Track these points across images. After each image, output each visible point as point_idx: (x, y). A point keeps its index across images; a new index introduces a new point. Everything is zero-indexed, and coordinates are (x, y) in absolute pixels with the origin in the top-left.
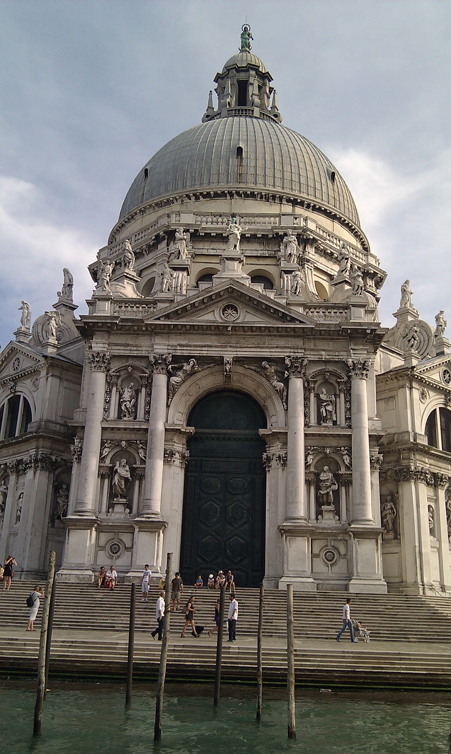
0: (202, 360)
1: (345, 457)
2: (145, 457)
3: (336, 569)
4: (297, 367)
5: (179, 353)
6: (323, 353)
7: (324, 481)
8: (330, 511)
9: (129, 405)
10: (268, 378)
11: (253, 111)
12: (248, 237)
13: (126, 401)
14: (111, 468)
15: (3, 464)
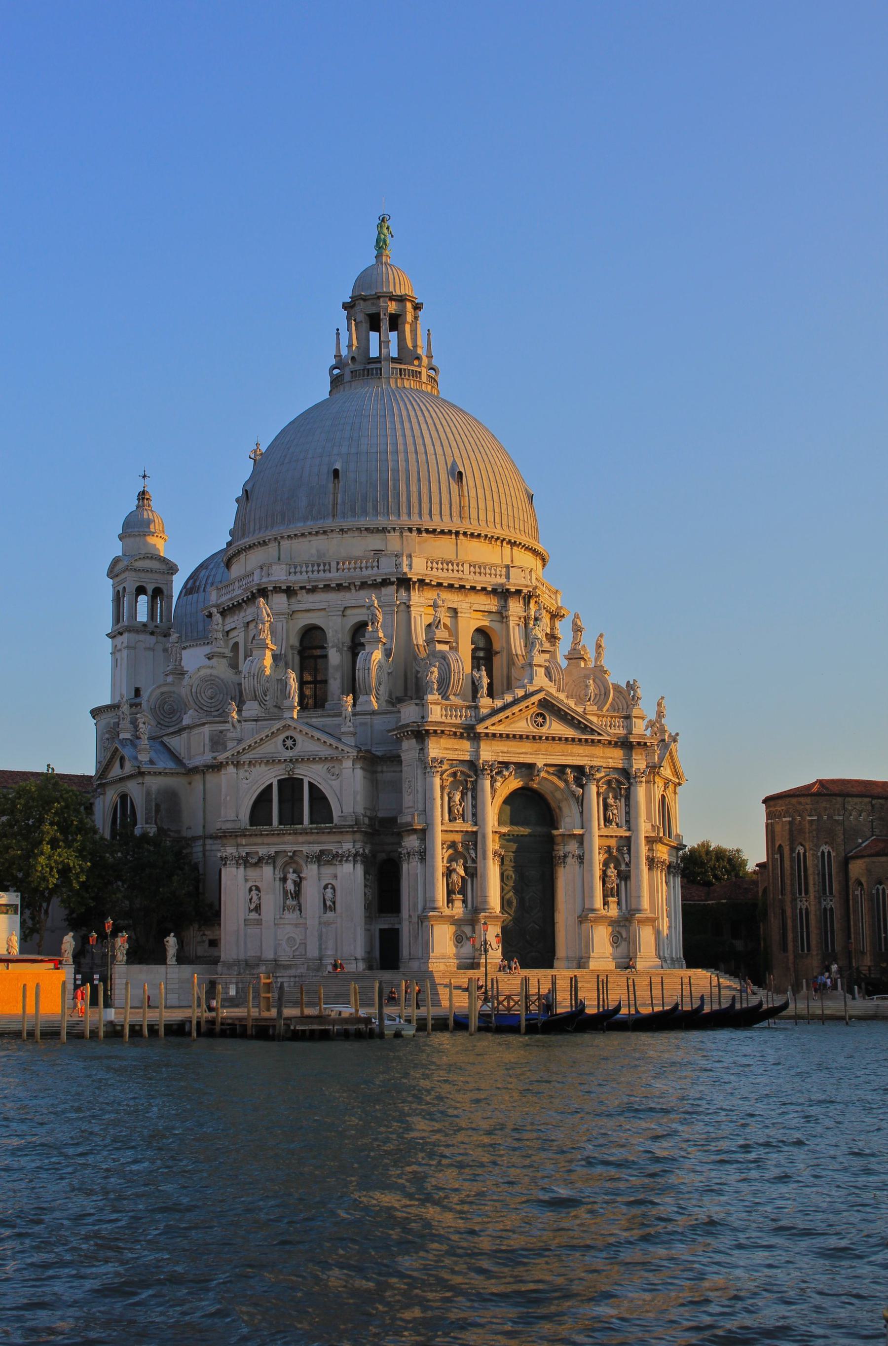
0: (519, 766)
1: (626, 856)
2: (476, 857)
3: (619, 950)
4: (593, 775)
5: (501, 759)
6: (610, 760)
7: (611, 877)
8: (614, 902)
9: (461, 809)
10: (566, 781)
11: (420, 373)
12: (478, 590)
13: (457, 805)
14: (448, 867)
15: (290, 852)
